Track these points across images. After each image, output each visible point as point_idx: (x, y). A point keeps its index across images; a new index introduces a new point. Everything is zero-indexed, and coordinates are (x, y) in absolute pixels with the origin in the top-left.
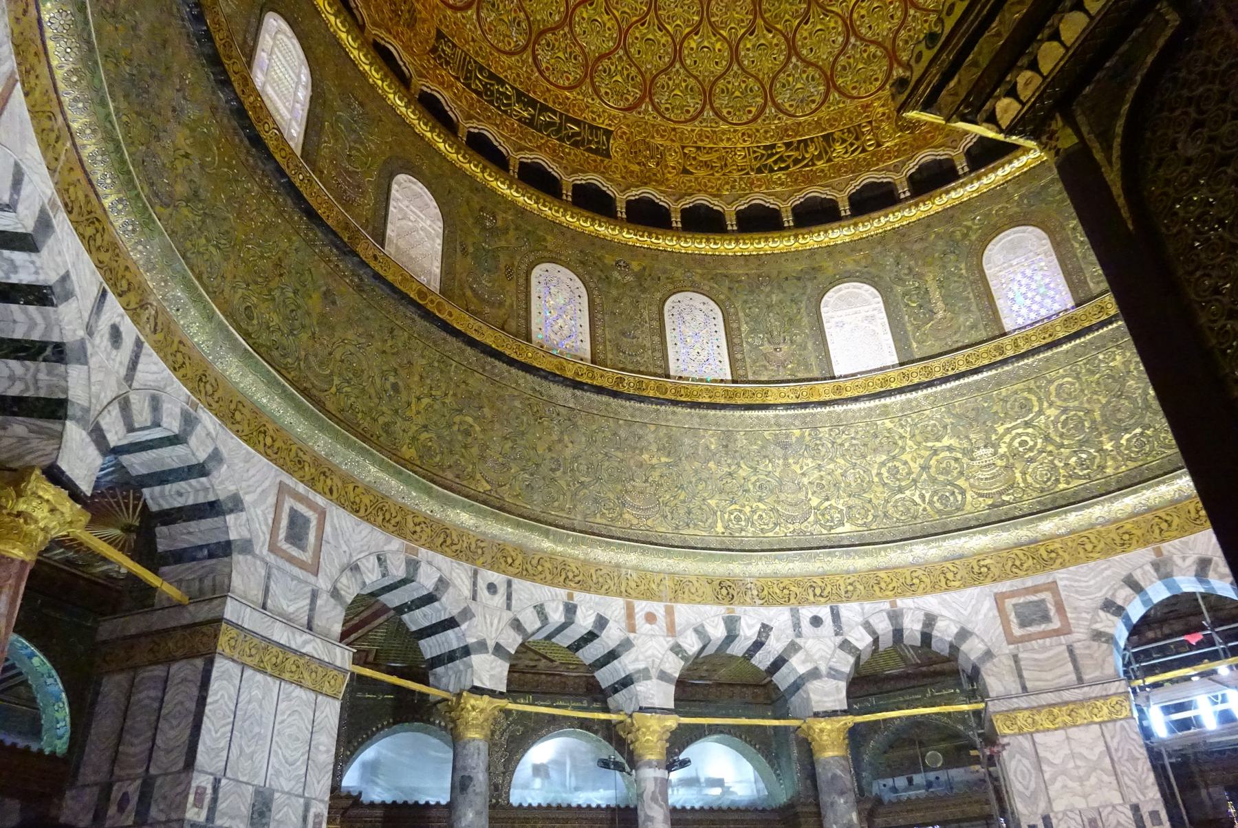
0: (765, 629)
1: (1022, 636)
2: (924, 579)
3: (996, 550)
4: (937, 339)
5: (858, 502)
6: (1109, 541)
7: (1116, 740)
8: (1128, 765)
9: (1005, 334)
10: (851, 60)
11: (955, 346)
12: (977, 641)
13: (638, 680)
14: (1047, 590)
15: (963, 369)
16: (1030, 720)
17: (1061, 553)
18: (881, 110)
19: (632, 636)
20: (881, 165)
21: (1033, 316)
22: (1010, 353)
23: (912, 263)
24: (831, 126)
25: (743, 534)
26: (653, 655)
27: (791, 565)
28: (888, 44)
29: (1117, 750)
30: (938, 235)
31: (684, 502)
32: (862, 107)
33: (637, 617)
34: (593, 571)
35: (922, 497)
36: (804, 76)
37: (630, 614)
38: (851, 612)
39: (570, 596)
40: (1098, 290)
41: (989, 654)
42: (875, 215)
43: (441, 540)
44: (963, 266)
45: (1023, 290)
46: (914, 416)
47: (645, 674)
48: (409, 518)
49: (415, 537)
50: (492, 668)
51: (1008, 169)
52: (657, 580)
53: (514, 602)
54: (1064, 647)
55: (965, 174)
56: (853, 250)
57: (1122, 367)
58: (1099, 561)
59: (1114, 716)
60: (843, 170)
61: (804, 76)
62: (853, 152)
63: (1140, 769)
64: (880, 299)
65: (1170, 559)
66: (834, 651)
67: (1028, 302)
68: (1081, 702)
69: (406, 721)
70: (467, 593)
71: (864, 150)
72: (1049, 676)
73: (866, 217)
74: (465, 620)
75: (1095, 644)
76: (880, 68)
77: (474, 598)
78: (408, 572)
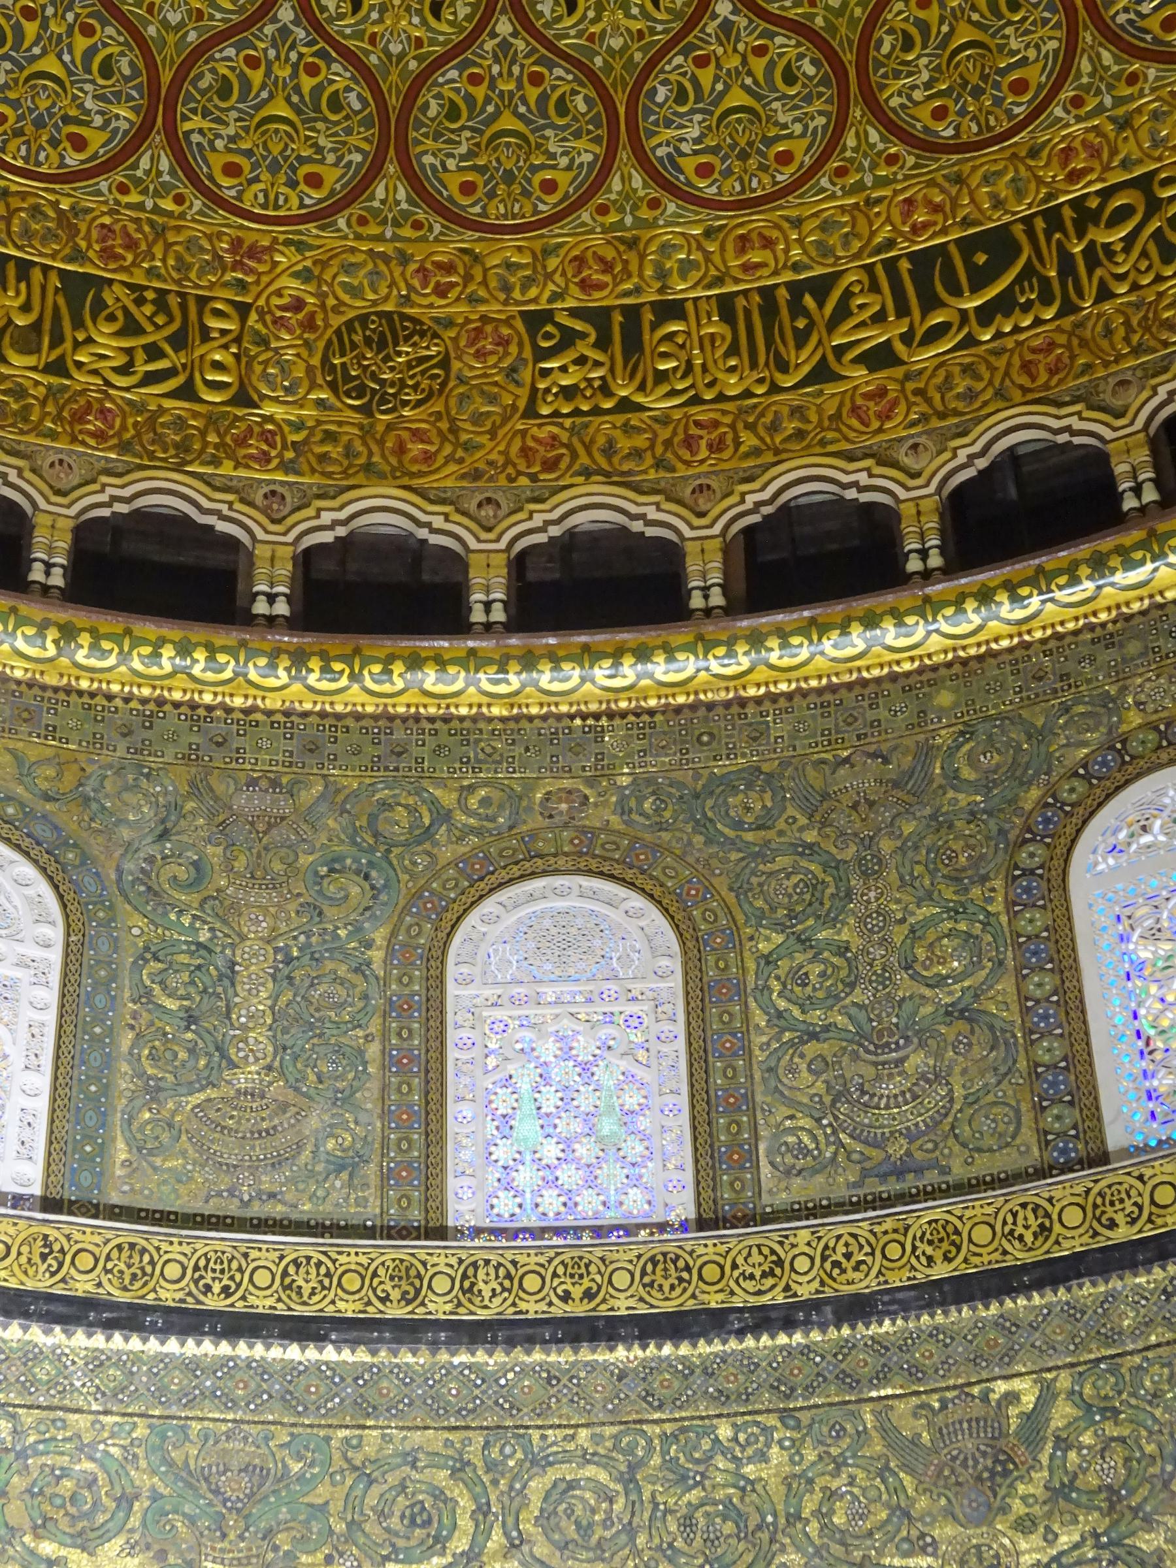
4: (207, 1158)
9: (440, 1232)
10: (257, 77)
11: (257, 1210)
15: (262, 1303)
18: (292, 286)
20: (227, 469)
21: (551, 1203)
22: (438, 1308)
23: (214, 853)
24: (108, 254)
28: (393, 84)
30: (332, 790)
32: (236, 244)
36: (82, 43)
40: (782, 1199)
42: (148, 629)
44: (380, 936)
45: (550, 1100)
46: (28, 1418)
51: (629, 672)
55: (488, 627)
56: (29, 716)
57: (776, 1489)
60: (94, 424)
61: (82, 43)
62: (150, 379)
64: (55, 933)
67: (551, 1151)
71: (187, 392)
73: (110, 623)
76: (340, 148)
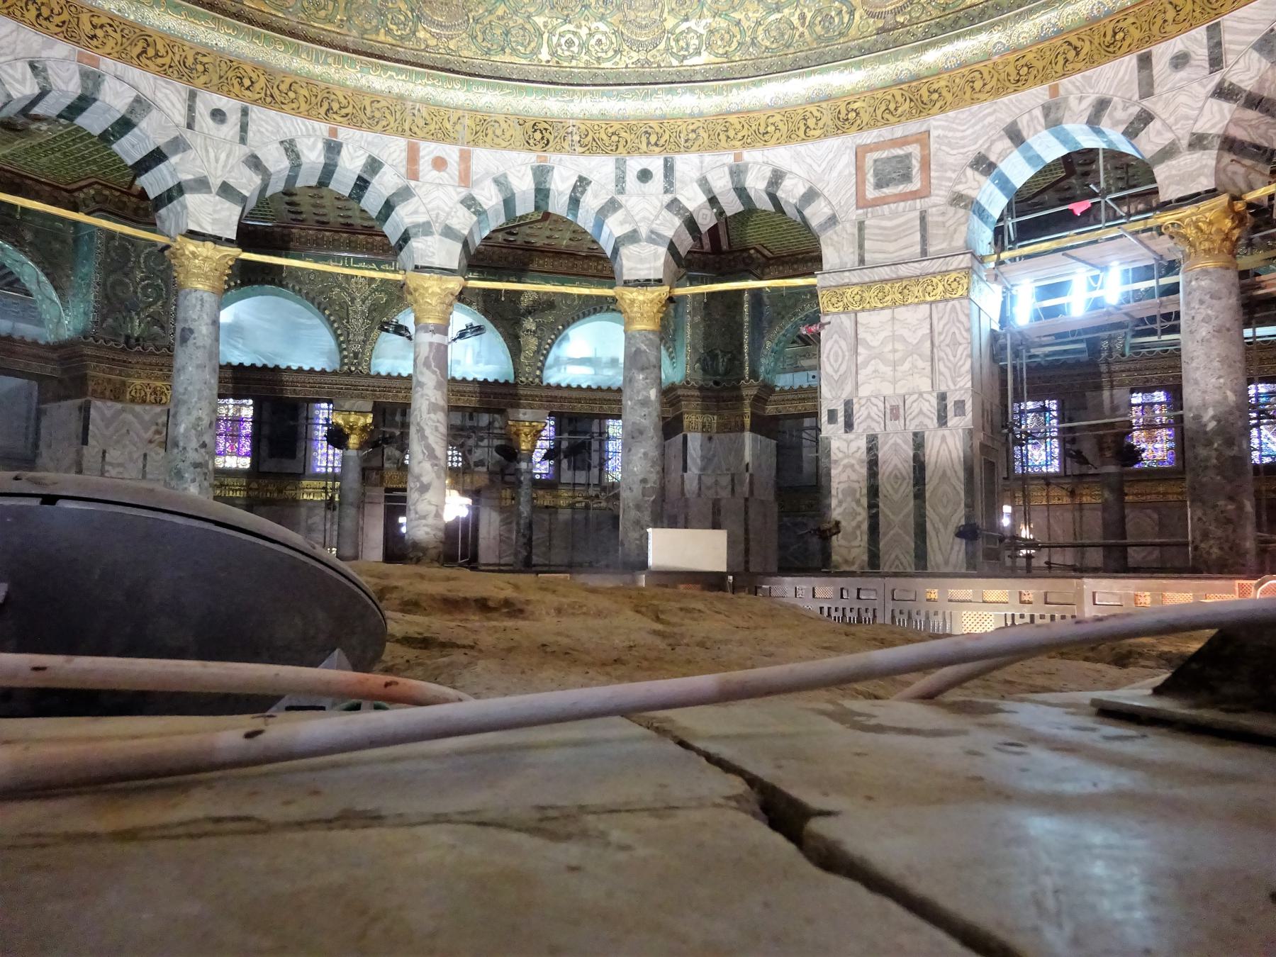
0: (583, 182)
1: (874, 199)
2: (781, 125)
3: (872, 89)
5: (724, 24)
6: (1003, 76)
7: (942, 322)
8: (948, 350)
12: (823, 204)
13: (416, 235)
14: (917, 141)
16: (858, 298)
17: (944, 93)
19: (413, 183)
25: (574, 63)
26: (438, 208)
27: (621, 104)
29: (940, 334)
31: (500, 18)
33: (421, 162)
34: (367, 103)
35: (802, 17)
37: (413, 156)
38: (687, 165)
39: (333, 132)
41: (832, 220)
43: (138, 50)
47: (426, 229)
48: (85, 18)
49: (95, 42)
50: (215, 211)
52: (453, 119)
53: (250, 134)
54: (918, 213)
58: (986, 103)
59: (948, 295)
63: (958, 356)
65: (1066, 99)
66: (660, 213)
68: (917, 278)
69: (255, 282)
70: (180, 117)
72: (891, 247)
74: (176, 152)
75: (952, 210)
77: (190, 126)
78: (84, 88)
